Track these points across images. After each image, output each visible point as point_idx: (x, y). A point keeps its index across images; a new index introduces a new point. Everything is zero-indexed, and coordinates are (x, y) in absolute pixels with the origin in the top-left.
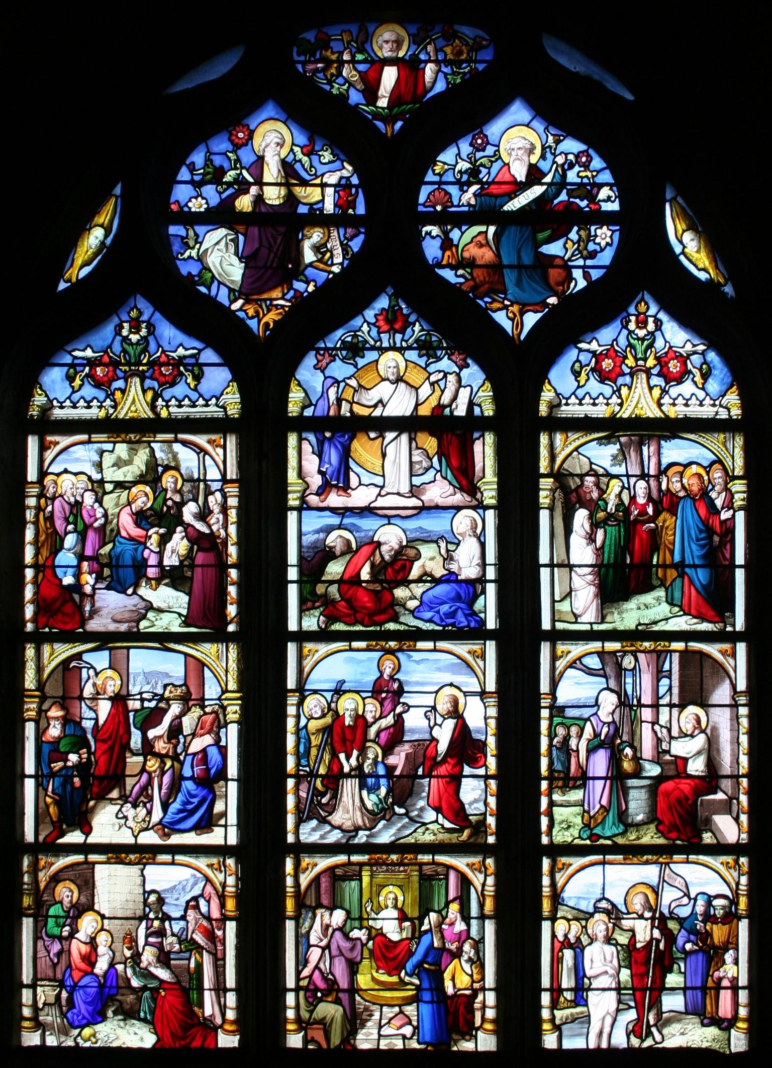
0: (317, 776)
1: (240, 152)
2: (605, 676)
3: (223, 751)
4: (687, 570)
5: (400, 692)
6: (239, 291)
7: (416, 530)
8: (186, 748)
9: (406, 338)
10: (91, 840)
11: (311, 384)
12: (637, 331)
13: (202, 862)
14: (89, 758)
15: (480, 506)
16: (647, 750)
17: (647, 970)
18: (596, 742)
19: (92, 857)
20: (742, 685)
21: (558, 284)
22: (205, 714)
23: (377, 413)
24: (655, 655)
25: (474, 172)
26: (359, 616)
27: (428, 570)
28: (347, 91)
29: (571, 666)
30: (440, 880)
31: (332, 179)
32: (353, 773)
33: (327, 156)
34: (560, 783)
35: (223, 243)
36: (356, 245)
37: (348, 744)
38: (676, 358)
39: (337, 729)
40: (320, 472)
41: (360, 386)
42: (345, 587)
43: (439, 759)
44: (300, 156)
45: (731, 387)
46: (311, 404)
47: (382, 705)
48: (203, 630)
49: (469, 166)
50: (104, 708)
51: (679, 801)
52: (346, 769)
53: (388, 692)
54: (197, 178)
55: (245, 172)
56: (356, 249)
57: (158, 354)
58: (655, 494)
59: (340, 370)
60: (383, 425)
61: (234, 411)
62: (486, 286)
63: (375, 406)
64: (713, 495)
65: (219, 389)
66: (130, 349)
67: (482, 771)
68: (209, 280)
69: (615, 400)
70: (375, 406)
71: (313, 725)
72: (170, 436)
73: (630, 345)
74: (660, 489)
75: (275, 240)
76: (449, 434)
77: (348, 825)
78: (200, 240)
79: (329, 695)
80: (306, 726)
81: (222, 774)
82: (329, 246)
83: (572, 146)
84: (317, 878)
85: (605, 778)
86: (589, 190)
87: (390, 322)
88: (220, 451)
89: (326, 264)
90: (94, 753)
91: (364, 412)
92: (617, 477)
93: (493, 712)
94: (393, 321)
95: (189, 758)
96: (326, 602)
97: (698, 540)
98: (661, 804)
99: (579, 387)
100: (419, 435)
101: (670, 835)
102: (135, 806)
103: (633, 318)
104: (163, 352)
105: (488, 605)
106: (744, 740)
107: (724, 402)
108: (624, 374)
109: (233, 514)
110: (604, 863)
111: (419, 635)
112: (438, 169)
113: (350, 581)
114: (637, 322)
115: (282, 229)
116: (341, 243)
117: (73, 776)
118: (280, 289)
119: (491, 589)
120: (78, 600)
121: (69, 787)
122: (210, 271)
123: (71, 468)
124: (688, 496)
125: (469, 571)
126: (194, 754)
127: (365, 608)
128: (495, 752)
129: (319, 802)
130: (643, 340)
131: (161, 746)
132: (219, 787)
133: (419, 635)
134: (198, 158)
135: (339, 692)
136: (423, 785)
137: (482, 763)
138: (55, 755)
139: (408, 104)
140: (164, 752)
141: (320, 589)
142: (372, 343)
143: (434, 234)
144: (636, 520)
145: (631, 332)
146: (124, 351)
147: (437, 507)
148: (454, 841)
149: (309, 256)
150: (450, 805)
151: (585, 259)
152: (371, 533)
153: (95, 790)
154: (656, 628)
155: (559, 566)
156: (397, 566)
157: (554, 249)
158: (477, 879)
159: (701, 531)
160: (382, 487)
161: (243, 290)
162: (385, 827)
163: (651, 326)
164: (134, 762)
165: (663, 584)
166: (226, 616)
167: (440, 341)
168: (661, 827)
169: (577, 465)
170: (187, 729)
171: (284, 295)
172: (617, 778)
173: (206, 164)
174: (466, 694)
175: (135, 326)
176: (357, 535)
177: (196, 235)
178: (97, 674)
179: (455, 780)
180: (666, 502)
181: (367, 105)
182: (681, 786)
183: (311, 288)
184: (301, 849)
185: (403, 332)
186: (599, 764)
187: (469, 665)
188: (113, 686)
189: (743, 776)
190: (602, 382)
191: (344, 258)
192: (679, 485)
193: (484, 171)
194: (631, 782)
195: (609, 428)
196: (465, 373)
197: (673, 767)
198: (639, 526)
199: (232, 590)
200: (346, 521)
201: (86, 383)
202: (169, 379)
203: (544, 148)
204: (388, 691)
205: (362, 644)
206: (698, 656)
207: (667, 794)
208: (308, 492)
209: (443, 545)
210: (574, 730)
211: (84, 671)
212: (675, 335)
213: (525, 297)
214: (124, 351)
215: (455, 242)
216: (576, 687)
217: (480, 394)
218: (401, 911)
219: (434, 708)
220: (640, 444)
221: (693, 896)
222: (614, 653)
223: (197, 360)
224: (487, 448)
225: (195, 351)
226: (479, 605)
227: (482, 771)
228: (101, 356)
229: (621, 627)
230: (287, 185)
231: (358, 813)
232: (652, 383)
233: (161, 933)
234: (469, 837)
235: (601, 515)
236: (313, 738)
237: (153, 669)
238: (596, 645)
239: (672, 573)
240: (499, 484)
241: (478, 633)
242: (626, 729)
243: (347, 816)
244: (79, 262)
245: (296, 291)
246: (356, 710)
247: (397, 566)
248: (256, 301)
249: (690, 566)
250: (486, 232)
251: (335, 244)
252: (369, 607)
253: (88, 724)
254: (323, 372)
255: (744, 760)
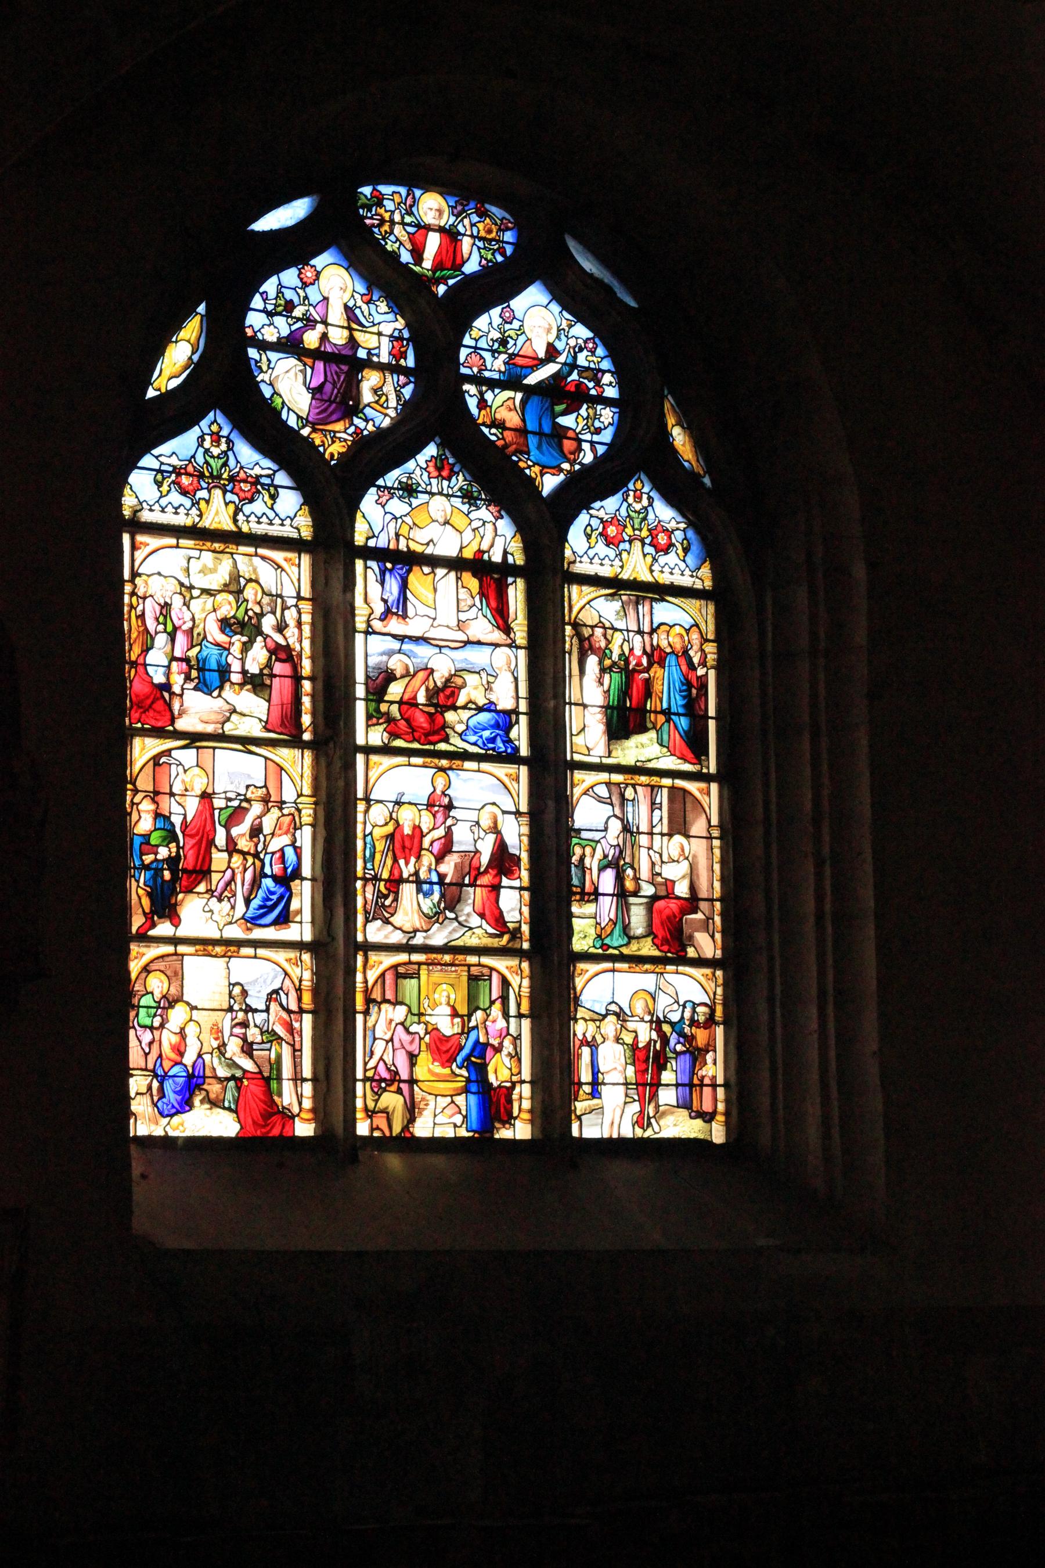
0: (381, 880)
1: (307, 289)
2: (612, 804)
3: (298, 851)
4: (673, 717)
5: (450, 807)
6: (307, 419)
7: (462, 661)
8: (265, 847)
9: (452, 485)
10: (182, 932)
11: (374, 518)
12: (634, 505)
13: (281, 956)
14: (178, 852)
15: (512, 645)
16: (645, 873)
17: (648, 1062)
18: (605, 862)
19: (182, 949)
20: (715, 821)
21: (571, 453)
22: (283, 815)
23: (429, 551)
24: (649, 789)
25: (503, 342)
26: (416, 735)
27: (473, 699)
28: (399, 248)
29: (585, 793)
30: (485, 980)
31: (387, 329)
32: (411, 879)
33: (383, 307)
34: (578, 897)
35: (292, 372)
36: (407, 392)
37: (407, 851)
38: (664, 531)
39: (398, 837)
40: (383, 600)
41: (414, 524)
42: (405, 707)
43: (482, 869)
44: (359, 303)
45: (705, 561)
46: (374, 536)
47: (434, 816)
48: (282, 737)
49: (500, 335)
50: (192, 805)
51: (668, 917)
52: (405, 875)
53: (440, 806)
54: (270, 308)
55: (311, 308)
56: (407, 397)
57: (237, 470)
58: (648, 649)
59: (397, 506)
60: (434, 562)
61: (307, 534)
62: (514, 446)
63: (428, 544)
64: (691, 653)
65: (288, 511)
66: (211, 461)
67: (516, 883)
68: (280, 406)
69: (617, 563)
70: (428, 544)
71: (378, 832)
72: (251, 550)
73: (629, 516)
74: (652, 645)
75: (339, 378)
76: (488, 574)
77: (408, 927)
78: (272, 366)
79: (390, 805)
80: (371, 834)
81: (297, 874)
82: (385, 389)
83: (581, 332)
84: (383, 975)
85: (613, 895)
86: (595, 375)
87: (439, 469)
88: (296, 569)
89: (382, 406)
90: (183, 848)
91: (419, 549)
92: (621, 630)
93: (525, 830)
94: (439, 465)
95: (268, 857)
96: (390, 720)
97: (681, 691)
98: (656, 921)
99: (590, 548)
100: (464, 574)
101: (663, 948)
102: (220, 900)
103: (631, 493)
104: (242, 468)
105: (521, 734)
106: (717, 867)
107: (700, 574)
108: (624, 541)
109: (307, 630)
110: (613, 970)
111: (466, 756)
112: (475, 333)
113: (407, 703)
114: (635, 497)
115: (345, 368)
116: (396, 391)
117: (163, 869)
118: (342, 422)
119: (523, 720)
120: (167, 698)
121: (159, 880)
122: (281, 397)
123: (158, 571)
124: (673, 652)
125: (506, 703)
126: (273, 853)
127: (422, 728)
128: (527, 867)
129: (383, 904)
130: (639, 513)
131: (244, 844)
132: (295, 885)
133: (466, 756)
134: (270, 286)
135: (398, 803)
136: (468, 893)
137: (516, 875)
138: (145, 848)
139: (449, 270)
140: (246, 849)
141: (384, 707)
142: (424, 486)
143: (471, 393)
144: (634, 670)
145: (630, 505)
146: (207, 462)
147: (479, 643)
148: (496, 945)
149: (367, 397)
150: (492, 913)
151: (592, 434)
152: (426, 661)
153: (184, 883)
154: (650, 765)
155: (576, 704)
156: (448, 692)
157: (567, 421)
158: (514, 980)
159: (683, 684)
160: (434, 619)
161: (310, 419)
162: (439, 930)
163: (645, 502)
164: (219, 859)
165: (654, 727)
166: (301, 725)
167: (479, 492)
168: (655, 940)
169: (588, 617)
170: (267, 829)
171: (346, 429)
172: (622, 895)
173: (277, 296)
174: (504, 812)
175: (216, 438)
176: (414, 660)
177: (269, 360)
178: (185, 771)
179: (495, 889)
180: (656, 657)
181: (415, 265)
182: (671, 905)
183: (370, 427)
184: (368, 947)
185: (449, 479)
186: (607, 882)
187: (506, 787)
188: (199, 784)
189: (717, 900)
190: (607, 545)
191: (398, 404)
192: (666, 642)
193: (511, 342)
194: (632, 900)
195: (615, 585)
196: (500, 523)
197: (664, 888)
198: (636, 675)
199: (306, 701)
200: (405, 647)
201: (173, 489)
202: (249, 495)
203: (559, 331)
204: (441, 806)
205: (419, 761)
206: (681, 793)
207: (660, 912)
208: (372, 617)
209: (484, 675)
210: (588, 850)
211: (173, 767)
212: (664, 513)
213: (545, 460)
214: (207, 462)
215: (489, 403)
216: (589, 813)
217: (512, 544)
218: (453, 1008)
219: (477, 823)
220: (637, 603)
221: (681, 1003)
222: (618, 784)
223: (272, 481)
224: (518, 593)
225: (271, 472)
226: (513, 734)
227: (516, 883)
228: (187, 465)
229: (624, 763)
230: (350, 329)
231: (416, 916)
232: (646, 552)
233: (245, 1025)
234: (508, 942)
235: (607, 662)
236: (377, 844)
237: (236, 772)
238: (604, 776)
239: (661, 718)
240: (529, 626)
241: (512, 757)
242: (628, 852)
243: (407, 918)
244: (166, 374)
245: (357, 427)
246: (413, 820)
247: (448, 692)
248: (322, 430)
249: (675, 714)
250: (514, 399)
251: (389, 389)
252: (424, 728)
253: (177, 820)
254: (383, 507)
255: (717, 885)
